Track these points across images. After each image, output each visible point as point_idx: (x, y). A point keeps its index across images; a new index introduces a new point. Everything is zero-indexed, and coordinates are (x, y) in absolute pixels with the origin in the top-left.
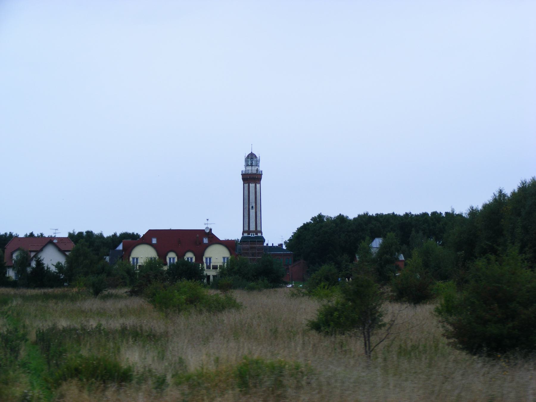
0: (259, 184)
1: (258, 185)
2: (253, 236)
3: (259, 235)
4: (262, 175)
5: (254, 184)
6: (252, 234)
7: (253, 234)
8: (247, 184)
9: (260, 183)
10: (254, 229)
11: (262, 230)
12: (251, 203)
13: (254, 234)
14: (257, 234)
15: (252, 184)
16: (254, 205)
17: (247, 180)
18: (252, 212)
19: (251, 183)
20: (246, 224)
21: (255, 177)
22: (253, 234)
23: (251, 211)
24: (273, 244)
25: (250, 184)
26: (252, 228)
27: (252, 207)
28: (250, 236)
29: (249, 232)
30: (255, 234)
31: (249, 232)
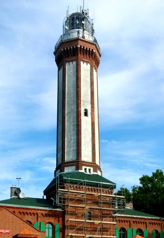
2: (88, 173)
3: (99, 173)
5: (89, 65)
6: (85, 169)
7: (88, 168)
8: (75, 63)
10: (90, 160)
12: (84, 101)
13: (90, 170)
15: (85, 63)
16: (89, 108)
19: (84, 61)
20: (71, 148)
22: (88, 170)
23: (83, 117)
25: (82, 63)
26: (86, 156)
27: (86, 110)
28: (83, 171)
30: (92, 169)
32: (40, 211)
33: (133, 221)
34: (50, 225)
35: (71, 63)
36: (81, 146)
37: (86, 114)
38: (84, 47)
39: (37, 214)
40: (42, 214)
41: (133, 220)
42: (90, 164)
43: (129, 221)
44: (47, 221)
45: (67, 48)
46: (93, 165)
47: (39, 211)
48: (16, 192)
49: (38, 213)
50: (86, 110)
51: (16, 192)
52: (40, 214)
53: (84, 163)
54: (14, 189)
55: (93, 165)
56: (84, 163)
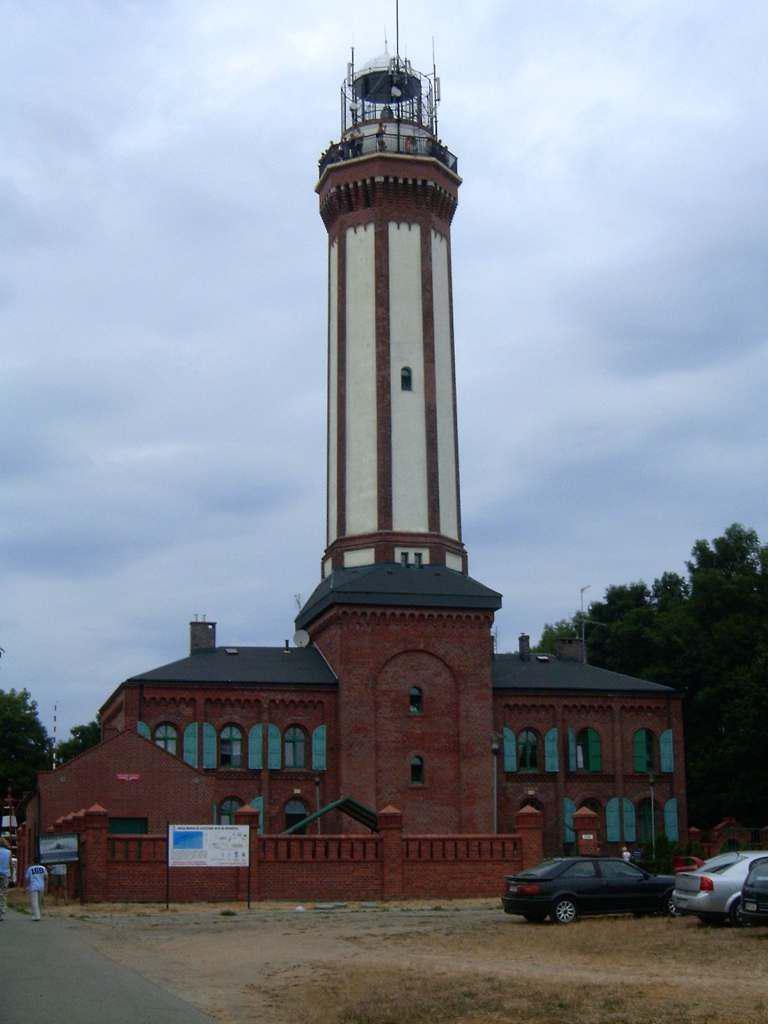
0: (444, 242)
1: (437, 243)
4: (458, 182)
5: (416, 230)
6: (405, 555)
7: (412, 553)
8: (371, 228)
9: (446, 236)
11: (463, 541)
14: (438, 559)
15: (404, 227)
17: (368, 204)
18: (408, 409)
21: (424, 182)
22: (412, 559)
24: (524, 640)
25: (392, 227)
26: (410, 517)
29: (384, 540)
31: (384, 540)
32: (265, 695)
33: (566, 706)
34: (298, 730)
35: (361, 229)
36: (390, 486)
37: (407, 382)
38: (396, 179)
39: (257, 701)
40: (273, 701)
41: (565, 702)
42: (422, 539)
43: (552, 706)
44: (289, 721)
45: (347, 186)
46: (428, 540)
47: (262, 694)
48: (202, 633)
49: (260, 698)
50: (407, 370)
51: (202, 633)
52: (268, 701)
53: (400, 538)
54: (199, 628)
55: (428, 540)
56: (400, 538)
